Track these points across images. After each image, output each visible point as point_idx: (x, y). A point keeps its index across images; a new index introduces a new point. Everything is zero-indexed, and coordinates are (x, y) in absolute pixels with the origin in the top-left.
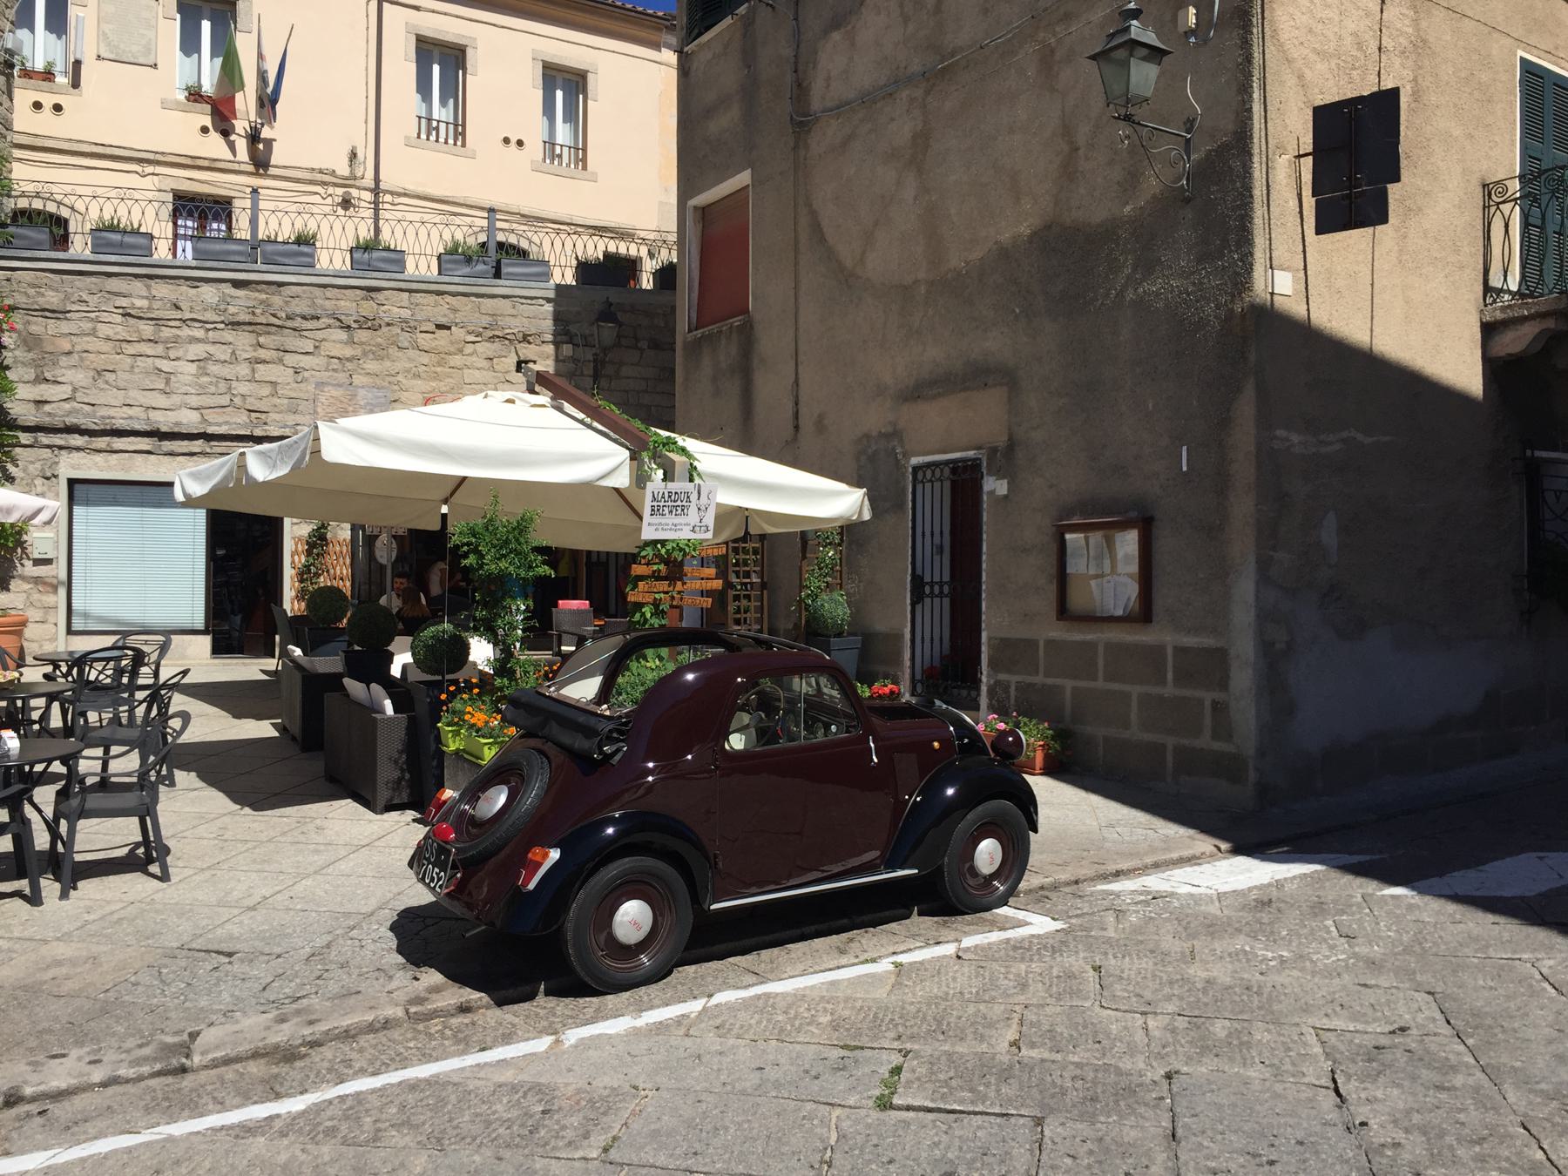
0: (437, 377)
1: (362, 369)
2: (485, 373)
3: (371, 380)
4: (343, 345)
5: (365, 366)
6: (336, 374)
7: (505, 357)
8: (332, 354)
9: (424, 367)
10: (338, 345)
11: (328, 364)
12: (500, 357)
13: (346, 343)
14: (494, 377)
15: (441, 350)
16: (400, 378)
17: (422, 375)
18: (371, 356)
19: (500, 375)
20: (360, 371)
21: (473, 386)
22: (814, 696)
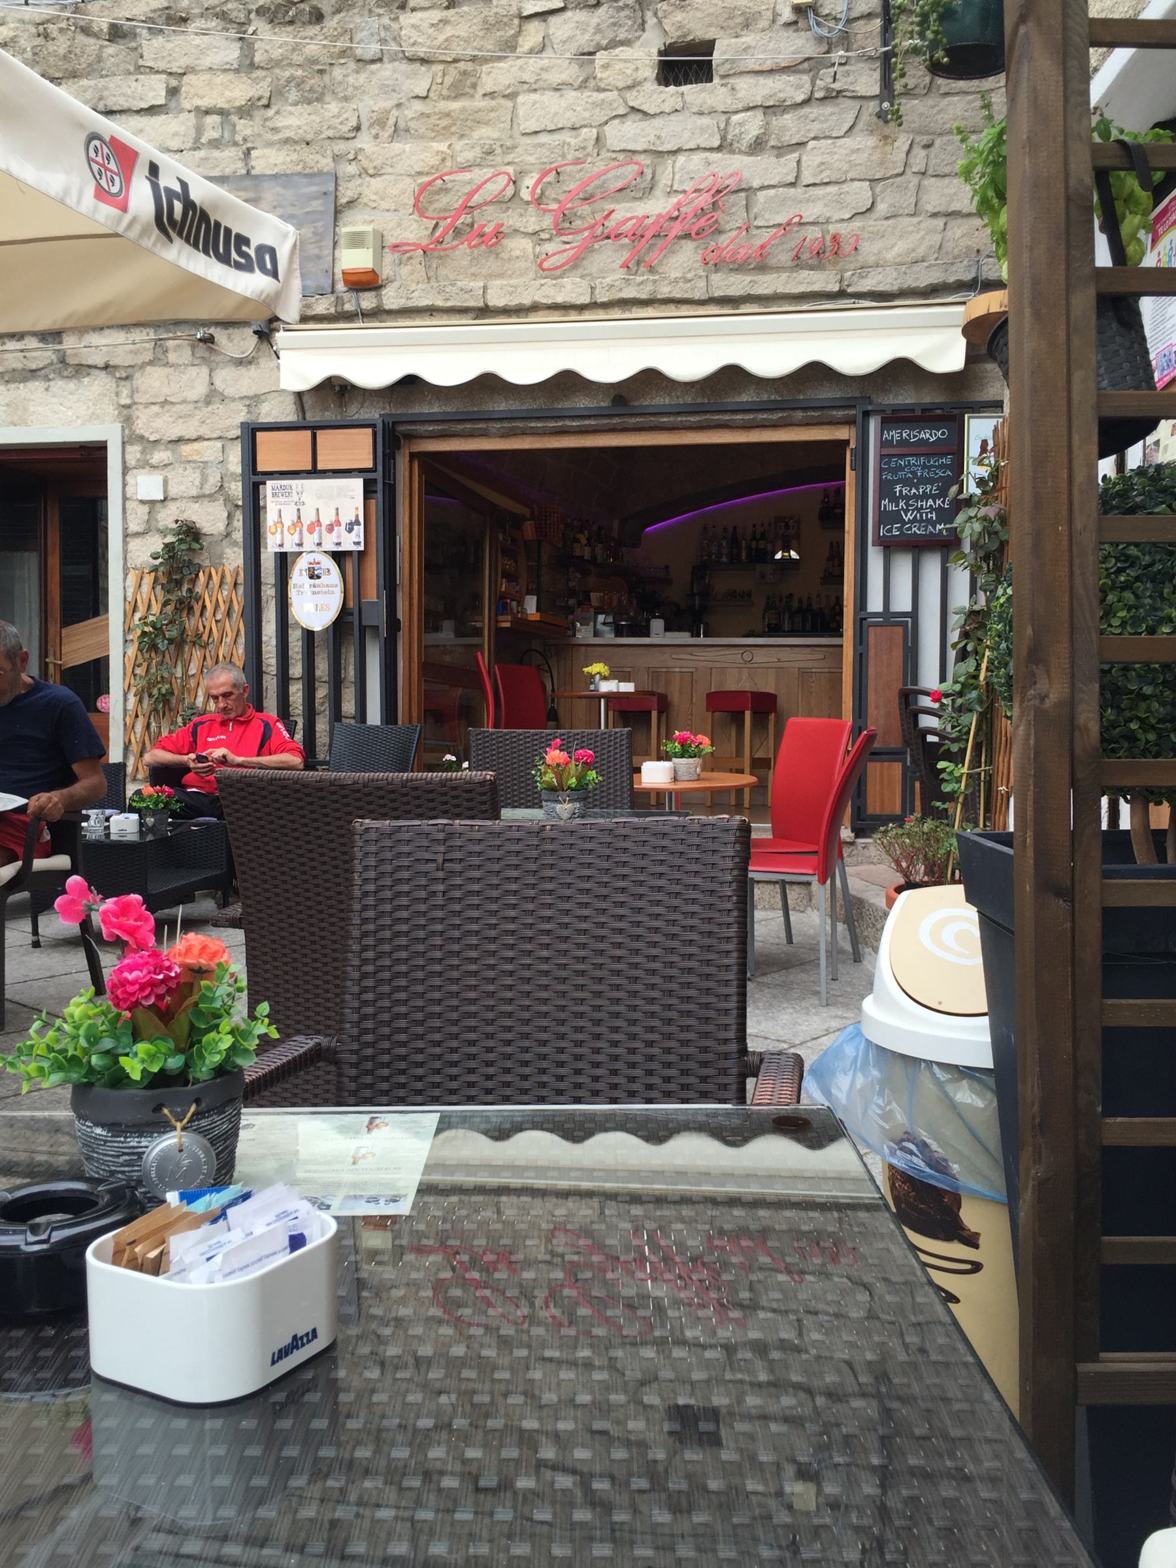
0: (450, 126)
1: (275, 130)
2: (571, 95)
3: (294, 156)
4: (231, 76)
5: (280, 122)
6: (216, 154)
7: (626, 43)
8: (204, 103)
9: (418, 106)
10: (221, 78)
11: (199, 130)
12: (613, 44)
13: (237, 71)
14: (595, 104)
15: (457, 51)
16: (364, 141)
17: (420, 127)
18: (293, 95)
19: (612, 96)
20: (269, 136)
21: (544, 138)
22: (904, 762)
